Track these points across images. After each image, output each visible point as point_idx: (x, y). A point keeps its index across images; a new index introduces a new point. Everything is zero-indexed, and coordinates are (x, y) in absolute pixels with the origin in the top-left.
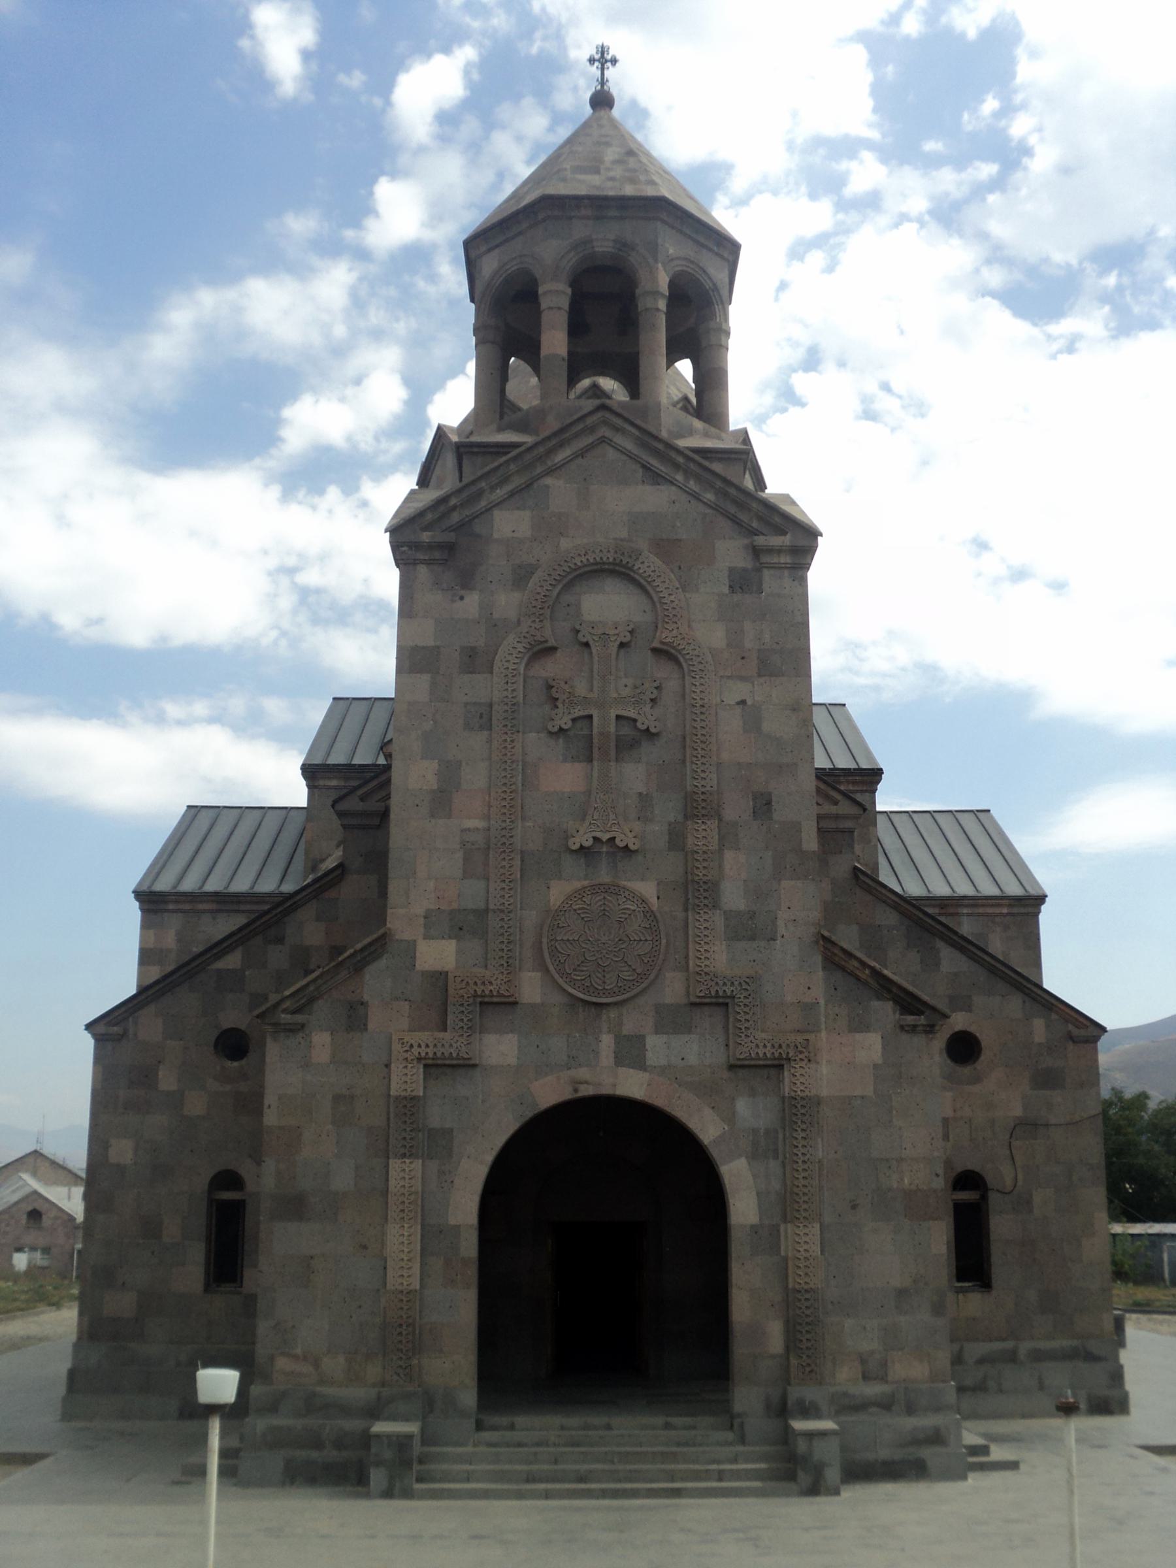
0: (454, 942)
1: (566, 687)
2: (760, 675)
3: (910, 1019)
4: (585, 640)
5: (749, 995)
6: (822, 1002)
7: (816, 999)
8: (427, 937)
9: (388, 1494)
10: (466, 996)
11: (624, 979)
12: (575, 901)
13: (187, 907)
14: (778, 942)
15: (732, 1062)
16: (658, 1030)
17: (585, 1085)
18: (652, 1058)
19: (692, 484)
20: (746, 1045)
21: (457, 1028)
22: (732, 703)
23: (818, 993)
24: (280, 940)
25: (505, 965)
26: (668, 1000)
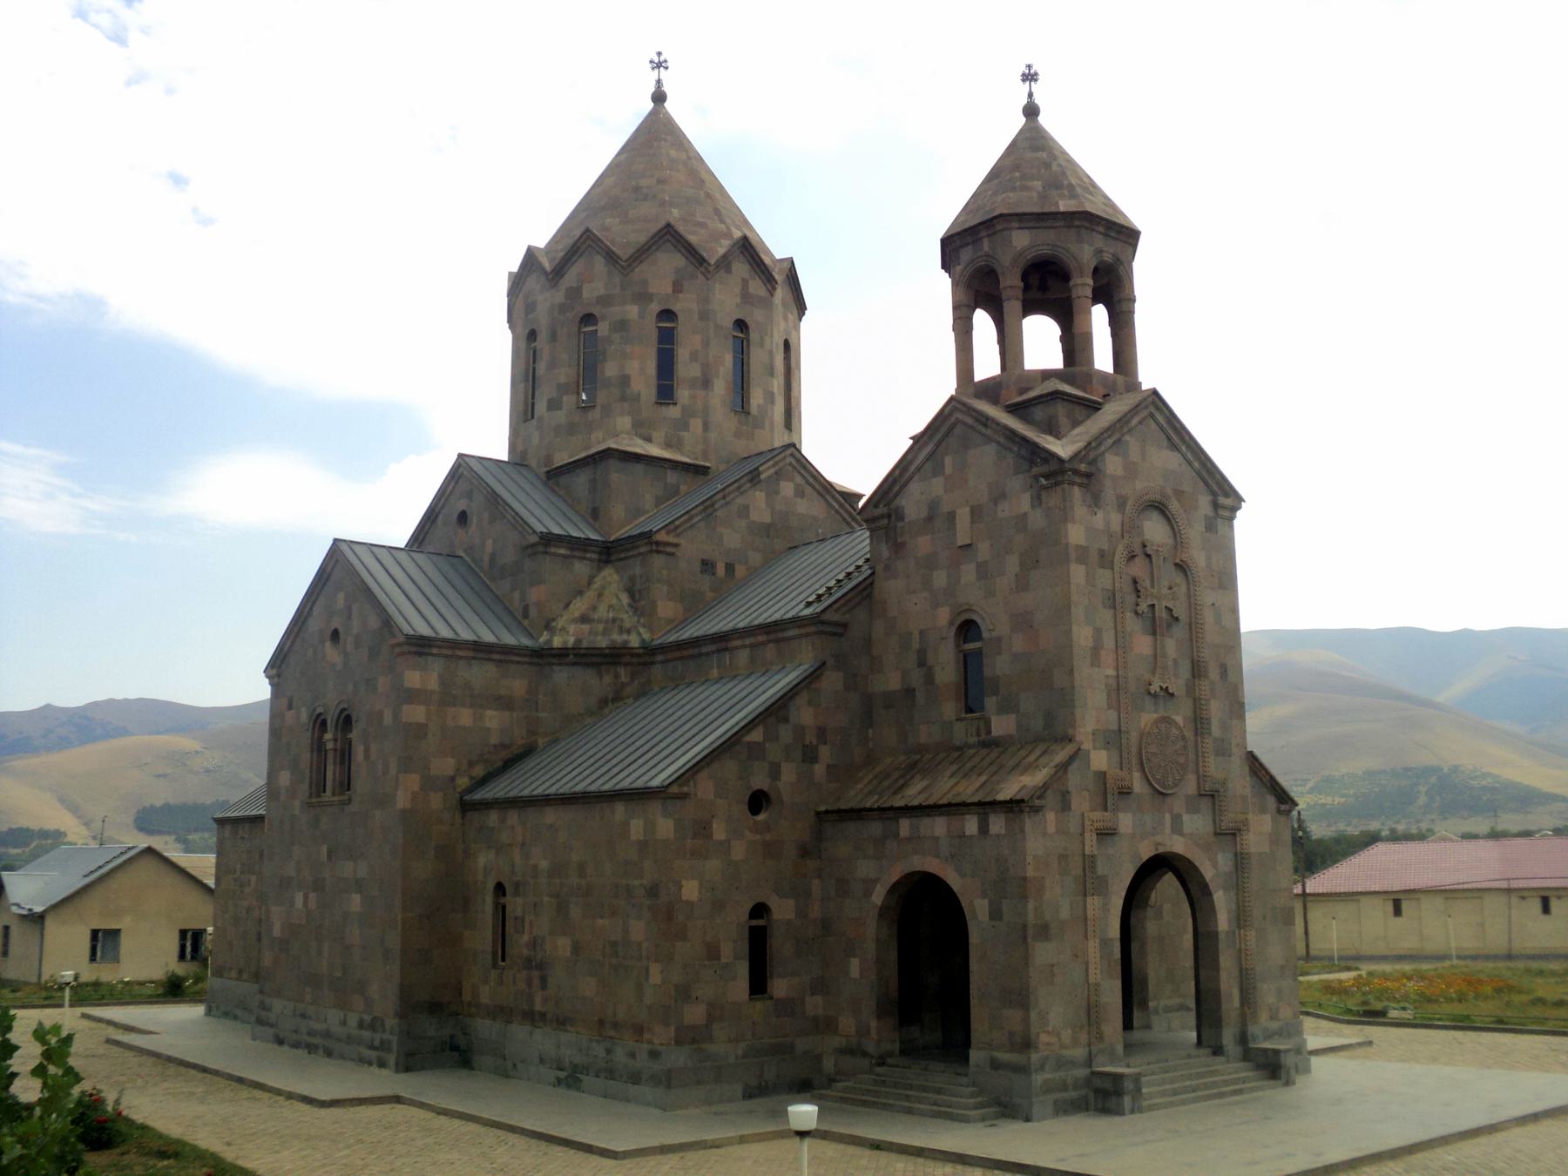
4: (1149, 553)
6: (1249, 795)
9: (1132, 1112)
13: (449, 652)
15: (1218, 831)
19: (1189, 456)
22: (1209, 604)
23: (1248, 791)
24: (786, 720)
26: (1190, 793)
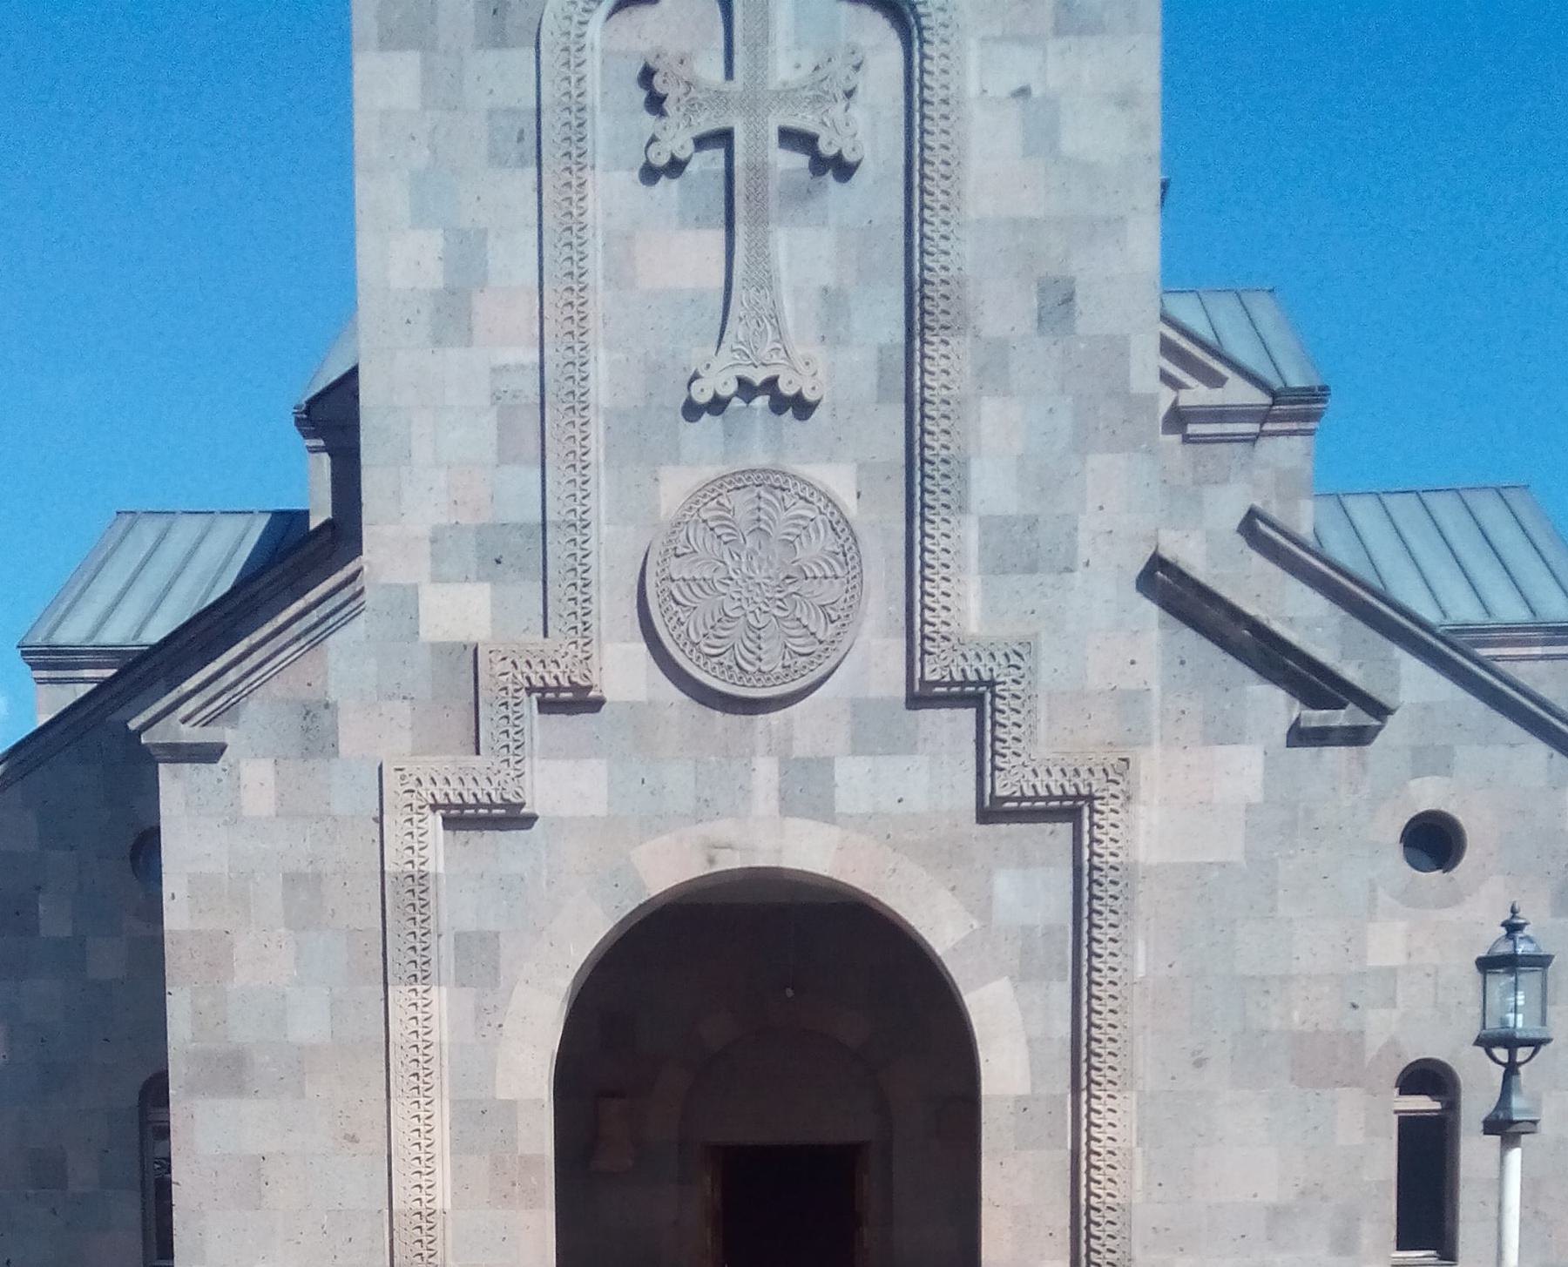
0: (486, 587)
1: (681, 71)
2: (1059, 31)
3: (1316, 718)
5: (1022, 677)
6: (1156, 688)
7: (1146, 683)
8: (437, 578)
10: (511, 687)
11: (794, 652)
12: (705, 504)
14: (1077, 574)
16: (859, 746)
17: (728, 850)
18: (844, 801)
20: (1014, 771)
21: (497, 747)
25: (580, 626)
